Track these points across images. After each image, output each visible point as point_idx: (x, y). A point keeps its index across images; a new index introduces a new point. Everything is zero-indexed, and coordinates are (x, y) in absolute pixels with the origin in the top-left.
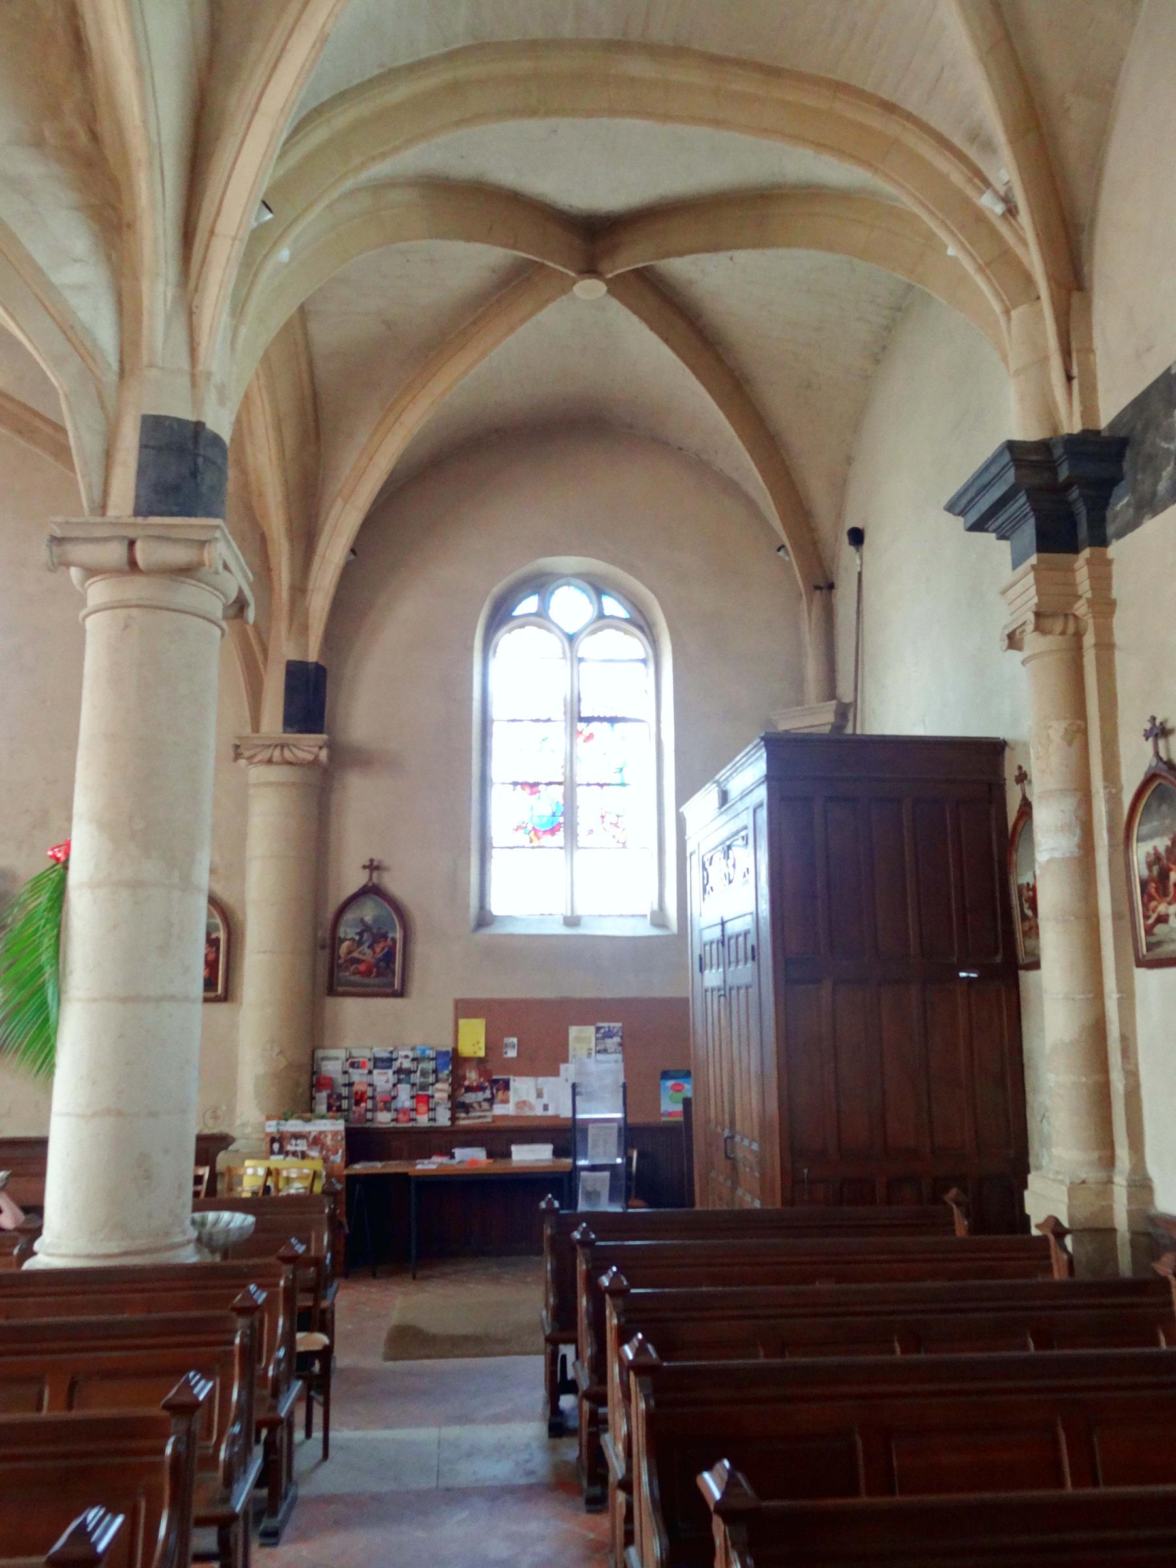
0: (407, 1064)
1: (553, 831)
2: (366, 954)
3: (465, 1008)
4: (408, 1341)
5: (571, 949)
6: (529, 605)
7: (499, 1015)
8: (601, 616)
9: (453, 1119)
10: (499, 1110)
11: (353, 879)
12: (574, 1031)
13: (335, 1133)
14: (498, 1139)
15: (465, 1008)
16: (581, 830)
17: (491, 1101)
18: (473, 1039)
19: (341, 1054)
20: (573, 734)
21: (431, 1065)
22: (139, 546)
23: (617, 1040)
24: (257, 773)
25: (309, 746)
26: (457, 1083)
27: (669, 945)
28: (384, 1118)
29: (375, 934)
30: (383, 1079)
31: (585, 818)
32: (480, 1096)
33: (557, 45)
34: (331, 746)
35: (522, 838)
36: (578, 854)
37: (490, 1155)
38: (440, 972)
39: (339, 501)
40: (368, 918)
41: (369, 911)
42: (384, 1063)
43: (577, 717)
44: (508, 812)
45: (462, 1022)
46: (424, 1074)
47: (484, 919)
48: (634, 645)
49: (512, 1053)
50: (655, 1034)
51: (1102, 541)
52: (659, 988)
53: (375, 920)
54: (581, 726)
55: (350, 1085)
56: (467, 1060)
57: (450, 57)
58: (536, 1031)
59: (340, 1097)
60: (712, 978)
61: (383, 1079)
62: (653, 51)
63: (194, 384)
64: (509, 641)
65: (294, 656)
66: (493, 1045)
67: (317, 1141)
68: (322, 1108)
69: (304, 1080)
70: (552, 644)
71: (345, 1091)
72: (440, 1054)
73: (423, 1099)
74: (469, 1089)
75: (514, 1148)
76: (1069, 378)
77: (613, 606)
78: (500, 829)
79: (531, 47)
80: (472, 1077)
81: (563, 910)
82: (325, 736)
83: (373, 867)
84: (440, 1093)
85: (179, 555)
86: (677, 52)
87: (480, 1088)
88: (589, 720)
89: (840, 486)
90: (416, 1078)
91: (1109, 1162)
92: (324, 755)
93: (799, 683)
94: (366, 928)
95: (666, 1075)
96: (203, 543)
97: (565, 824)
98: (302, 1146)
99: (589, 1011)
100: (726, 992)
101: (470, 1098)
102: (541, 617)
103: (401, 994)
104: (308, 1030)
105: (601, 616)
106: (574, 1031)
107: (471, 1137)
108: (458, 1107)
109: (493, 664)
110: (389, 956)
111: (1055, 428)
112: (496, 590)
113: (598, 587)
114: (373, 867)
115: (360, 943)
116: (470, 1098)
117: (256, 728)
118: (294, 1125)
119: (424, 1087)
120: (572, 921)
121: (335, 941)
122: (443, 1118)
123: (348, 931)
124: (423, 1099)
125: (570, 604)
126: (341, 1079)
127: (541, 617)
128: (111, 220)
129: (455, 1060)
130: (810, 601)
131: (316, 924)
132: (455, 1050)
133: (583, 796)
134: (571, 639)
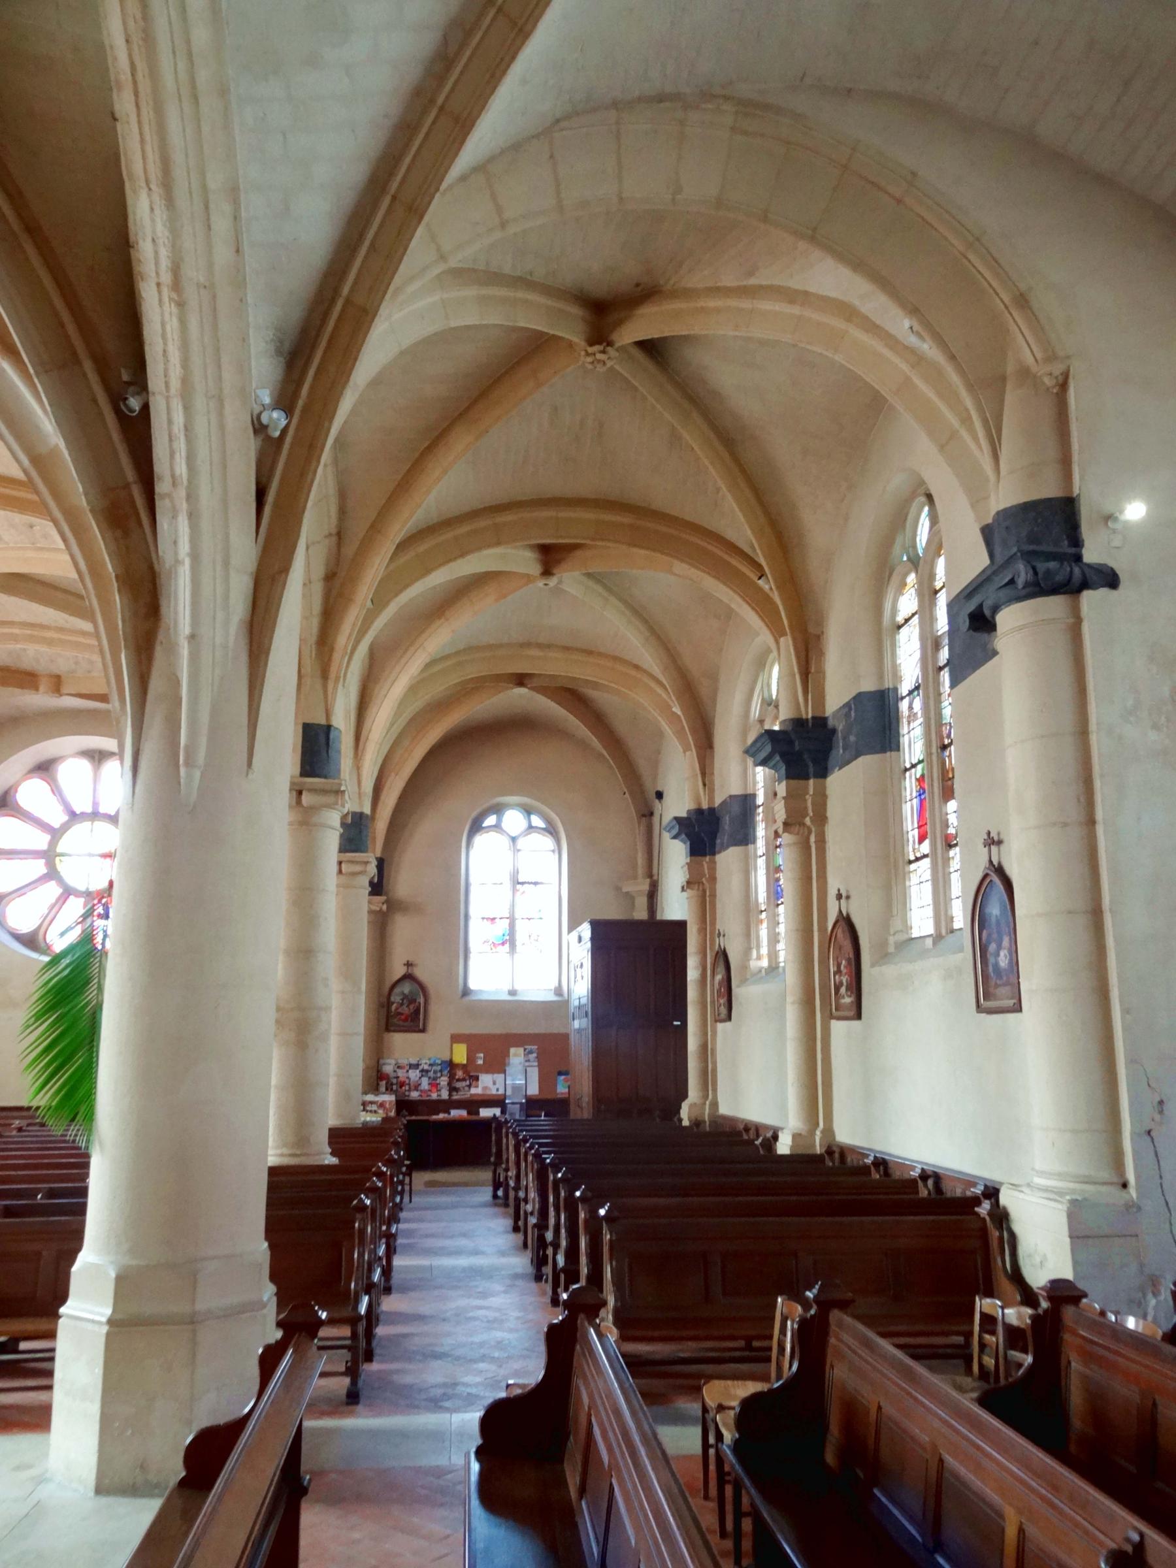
0: (426, 1067)
1: (503, 944)
3: (456, 1039)
4: (431, 1184)
5: (513, 1008)
6: (491, 820)
7: (474, 1042)
8: (531, 827)
9: (450, 1095)
10: (473, 1091)
11: (399, 971)
12: (512, 1050)
13: (390, 1102)
14: (473, 1105)
15: (456, 1039)
16: (518, 943)
17: (470, 1086)
18: (460, 1055)
19: (393, 1062)
20: (514, 890)
21: (439, 1068)
22: (343, 865)
23: (535, 1055)
26: (452, 1077)
27: (558, 1007)
28: (415, 1095)
29: (410, 1000)
30: (414, 1075)
31: (520, 937)
32: (464, 1084)
33: (501, 646)
34: (387, 902)
35: (487, 947)
36: (516, 956)
37: (469, 1113)
38: (443, 1020)
39: (393, 774)
40: (406, 991)
41: (406, 988)
42: (416, 1066)
43: (516, 882)
44: (480, 934)
45: (455, 1046)
46: (435, 1072)
47: (466, 992)
48: (548, 842)
49: (480, 1062)
50: (551, 1050)
51: (713, 854)
52: (555, 1028)
53: (411, 992)
54: (519, 886)
55: (397, 1077)
56: (457, 1065)
57: (458, 653)
58: (492, 1050)
59: (392, 1084)
60: (576, 1024)
61: (414, 1075)
62: (540, 646)
63: (360, 797)
64: (480, 840)
66: (471, 1058)
67: (382, 1105)
68: (383, 1089)
69: (375, 1074)
70: (505, 841)
71: (394, 1081)
72: (443, 1062)
73: (434, 1085)
74: (458, 1080)
75: (481, 1110)
76: (704, 785)
77: (537, 821)
79: (490, 647)
80: (460, 1074)
81: (507, 987)
82: (383, 898)
83: (408, 964)
84: (444, 1081)
85: (358, 868)
86: (549, 646)
87: (464, 1080)
88: (522, 883)
90: (431, 1074)
91: (706, 1097)
92: (385, 907)
93: (634, 867)
94: (405, 997)
95: (560, 1074)
96: (367, 863)
97: (510, 941)
98: (374, 1107)
99: (519, 1040)
100: (579, 1031)
101: (459, 1085)
102: (497, 827)
103: (423, 1031)
104: (377, 1050)
105: (531, 827)
106: (512, 1050)
107: (459, 1104)
108: (452, 1089)
109: (472, 853)
110: (417, 1011)
111: (699, 804)
112: (474, 814)
113: (528, 811)
114: (408, 964)
115: (402, 1004)
118: (370, 1097)
119: (435, 1079)
120: (513, 993)
122: (445, 1095)
123: (396, 998)
124: (434, 1085)
125: (514, 820)
126: (392, 1075)
127: (497, 827)
129: (451, 1065)
130: (639, 823)
131: (380, 994)
132: (451, 1061)
133: (519, 925)
134: (514, 839)
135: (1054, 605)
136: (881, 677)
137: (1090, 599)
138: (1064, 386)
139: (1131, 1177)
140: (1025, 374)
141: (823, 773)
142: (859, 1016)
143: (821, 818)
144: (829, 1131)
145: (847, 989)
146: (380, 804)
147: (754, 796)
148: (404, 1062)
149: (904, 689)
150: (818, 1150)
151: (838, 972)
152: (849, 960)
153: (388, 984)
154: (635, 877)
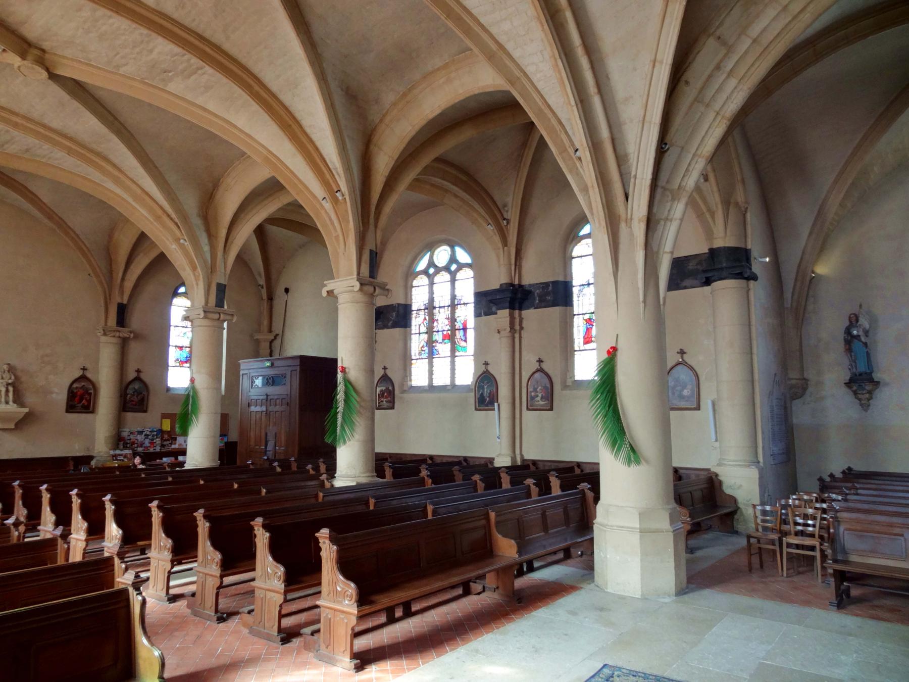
2: (135, 399)
3: (164, 416)
10: (173, 446)
11: (132, 375)
15: (164, 416)
17: (171, 444)
18: (166, 425)
24: (103, 339)
25: (124, 332)
29: (138, 392)
30: (140, 438)
38: (157, 406)
39: (142, 255)
40: (136, 387)
41: (137, 386)
42: (140, 433)
65: (120, 301)
66: (173, 427)
67: (125, 456)
68: (122, 447)
78: (171, 361)
80: (166, 436)
83: (138, 371)
84: (158, 441)
89: (280, 273)
94: (136, 391)
101: (165, 443)
104: (119, 423)
107: (167, 454)
108: (163, 446)
116: (165, 443)
117: (106, 324)
118: (118, 452)
119: (152, 440)
121: (126, 395)
122: (158, 449)
123: (130, 391)
124: (152, 443)
128: (211, 236)
129: (161, 432)
135: (743, 282)
136: (565, 276)
137: (752, 283)
138: (746, 211)
139: (761, 459)
140: (737, 204)
141: (520, 309)
142: (551, 409)
143: (522, 328)
144: (522, 456)
145: (542, 398)
146: (129, 271)
147: (411, 306)
148: (133, 430)
149: (575, 283)
150: (519, 463)
151: (535, 390)
152: (545, 387)
153: (125, 384)
154: (259, 331)
